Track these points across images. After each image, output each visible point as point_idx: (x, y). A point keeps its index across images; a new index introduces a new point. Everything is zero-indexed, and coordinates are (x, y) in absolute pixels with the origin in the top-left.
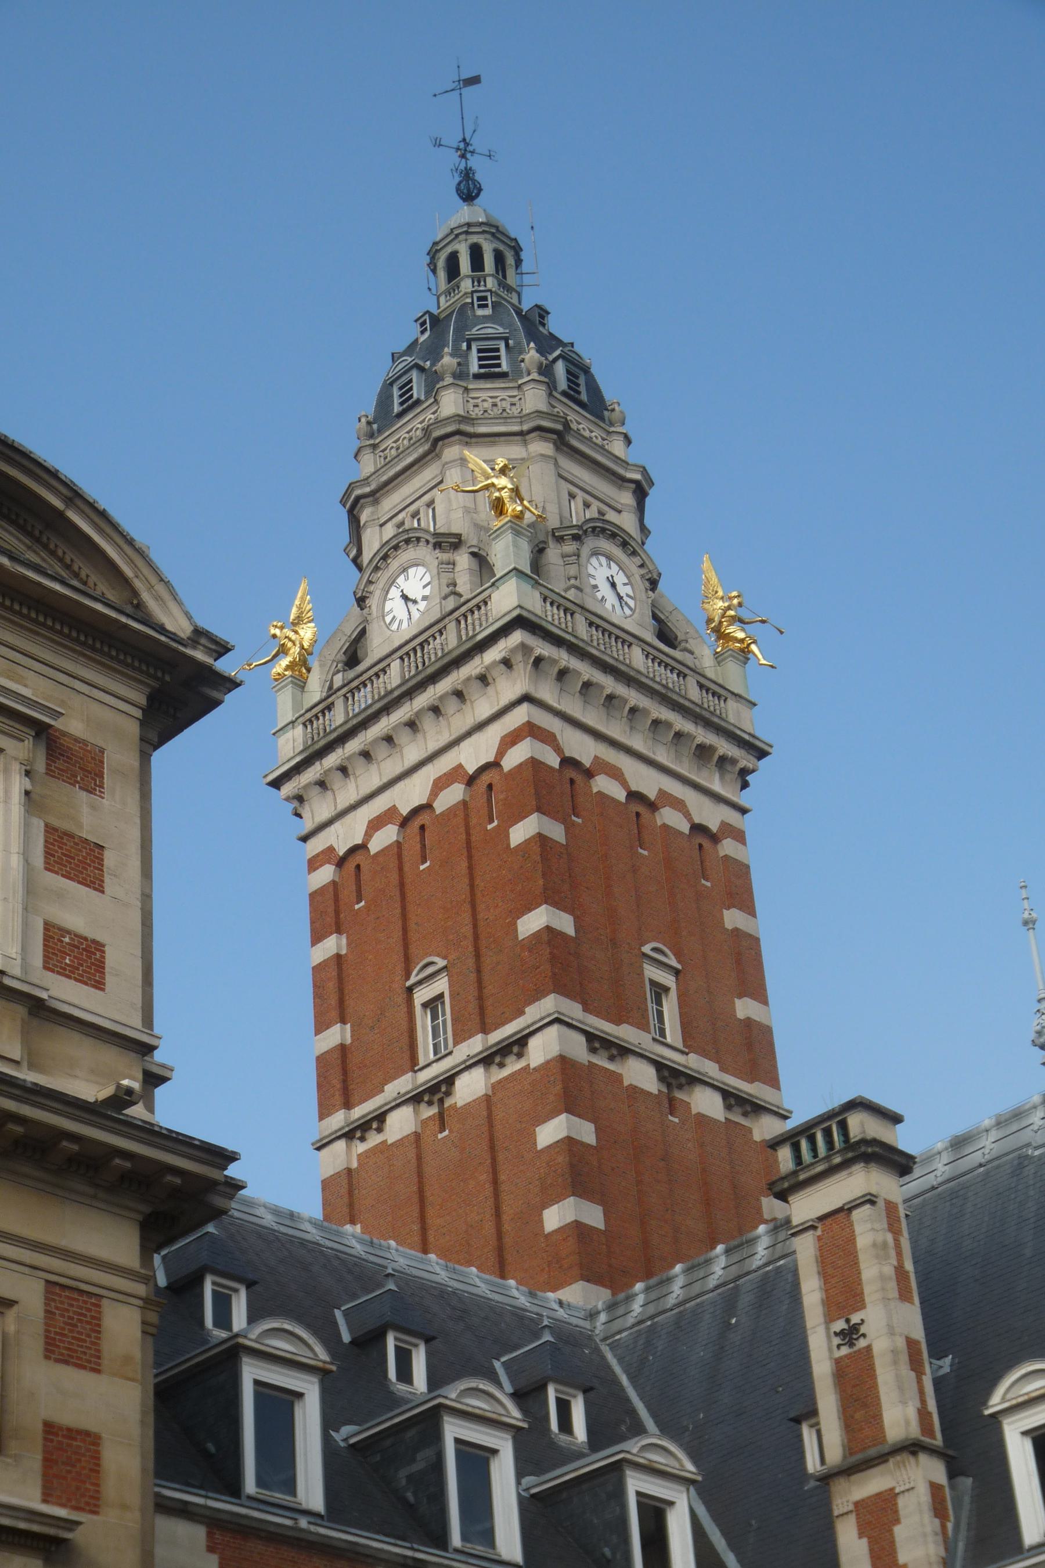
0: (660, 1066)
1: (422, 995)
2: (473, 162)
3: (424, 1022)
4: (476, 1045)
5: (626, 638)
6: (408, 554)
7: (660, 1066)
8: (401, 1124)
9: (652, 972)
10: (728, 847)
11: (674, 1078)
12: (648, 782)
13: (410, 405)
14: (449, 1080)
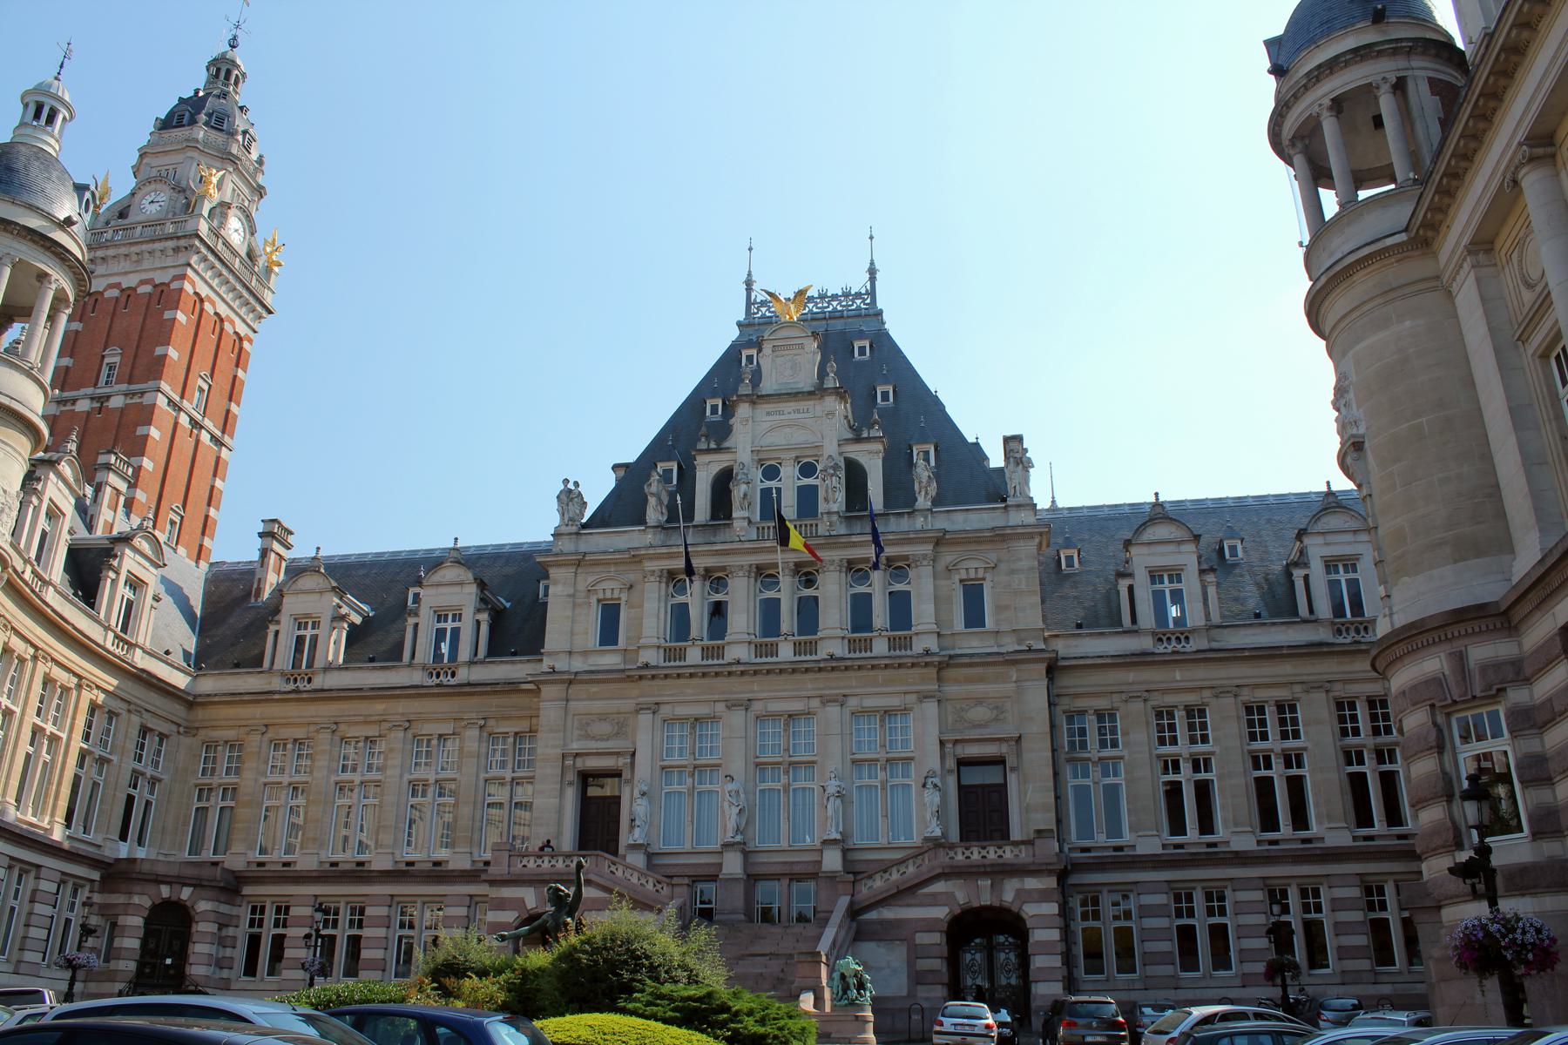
0: (192, 419)
1: (107, 360)
2: (239, 32)
3: (105, 371)
4: (124, 387)
5: (235, 253)
6: (159, 186)
7: (192, 419)
8: (83, 406)
9: (200, 382)
10: (246, 344)
11: (195, 424)
12: (223, 310)
13: (180, 125)
14: (108, 397)
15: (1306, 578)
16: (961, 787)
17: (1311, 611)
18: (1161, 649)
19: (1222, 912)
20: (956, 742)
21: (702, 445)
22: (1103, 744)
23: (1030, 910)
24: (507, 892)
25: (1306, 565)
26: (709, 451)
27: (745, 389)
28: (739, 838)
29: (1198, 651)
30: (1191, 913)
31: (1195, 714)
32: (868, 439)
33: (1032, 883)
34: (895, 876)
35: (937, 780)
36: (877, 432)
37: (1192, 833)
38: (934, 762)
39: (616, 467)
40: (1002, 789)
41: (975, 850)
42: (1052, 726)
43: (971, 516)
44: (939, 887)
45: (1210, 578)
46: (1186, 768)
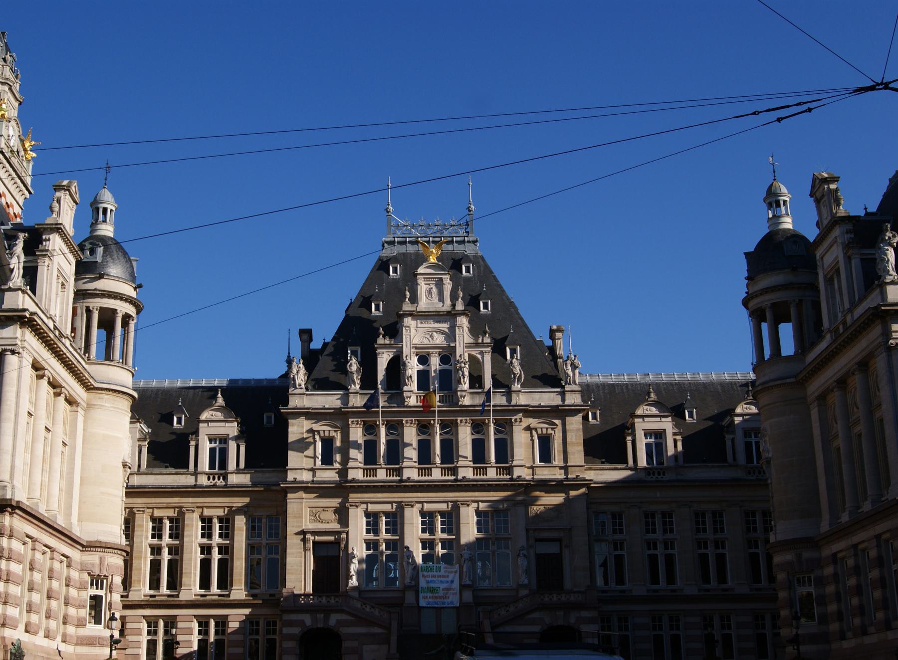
15: (733, 440)
16: (536, 554)
17: (735, 459)
18: (649, 478)
19: (678, 628)
20: (535, 530)
21: (381, 340)
22: (615, 532)
23: (585, 628)
24: (294, 617)
25: (733, 432)
26: (385, 346)
27: (407, 307)
28: (413, 583)
29: (669, 481)
30: (661, 629)
31: (667, 516)
32: (483, 345)
33: (585, 614)
34: (512, 609)
35: (525, 552)
37: (662, 583)
38: (522, 542)
40: (558, 557)
41: (555, 595)
42: (589, 521)
44: (536, 615)
45: (679, 437)
46: (660, 547)
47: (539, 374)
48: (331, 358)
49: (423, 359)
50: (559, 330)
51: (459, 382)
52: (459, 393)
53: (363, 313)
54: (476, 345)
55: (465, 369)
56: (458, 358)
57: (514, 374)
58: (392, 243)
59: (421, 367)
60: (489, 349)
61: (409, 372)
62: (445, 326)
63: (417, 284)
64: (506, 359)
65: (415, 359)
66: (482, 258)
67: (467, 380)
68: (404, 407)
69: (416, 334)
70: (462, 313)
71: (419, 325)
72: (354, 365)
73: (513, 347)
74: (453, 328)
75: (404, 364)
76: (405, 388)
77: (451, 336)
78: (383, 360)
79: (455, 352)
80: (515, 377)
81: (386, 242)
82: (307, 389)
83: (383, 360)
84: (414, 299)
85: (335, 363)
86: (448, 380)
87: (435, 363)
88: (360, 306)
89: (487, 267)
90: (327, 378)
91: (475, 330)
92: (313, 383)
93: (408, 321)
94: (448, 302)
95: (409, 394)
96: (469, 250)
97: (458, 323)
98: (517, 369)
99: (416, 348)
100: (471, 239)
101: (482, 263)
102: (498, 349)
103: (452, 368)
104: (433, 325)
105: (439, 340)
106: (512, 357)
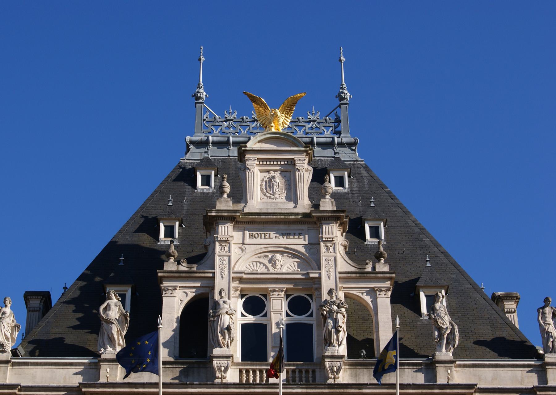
21: (170, 266)
26: (178, 276)
32: (374, 276)
36: (382, 267)
39: (28, 296)
43: (502, 372)
47: (489, 337)
48: (73, 307)
49: (255, 304)
50: (509, 297)
51: (328, 342)
52: (328, 363)
53: (145, 240)
54: (361, 276)
55: (340, 316)
56: (325, 296)
57: (440, 329)
58: (203, 144)
59: (250, 319)
60: (388, 284)
61: (226, 320)
62: (298, 243)
63: (246, 169)
64: (419, 313)
65: (238, 304)
66: (366, 167)
67: (343, 336)
68: (214, 385)
69: (239, 255)
70: (333, 217)
71: (247, 241)
72: (114, 309)
73: (432, 292)
74: (314, 247)
75: (216, 305)
76: (217, 351)
77: (311, 259)
78: (175, 303)
79: (319, 289)
80: (441, 336)
81: (193, 143)
82: (15, 353)
83: (175, 303)
84: (239, 194)
85: (80, 315)
86: (302, 343)
87: (278, 312)
88: (137, 231)
89: (374, 180)
90: (62, 339)
91: (357, 251)
92: (32, 347)
93: (225, 230)
94: (304, 204)
95: (224, 362)
96: (345, 154)
97: (325, 236)
98: (446, 321)
99: (241, 280)
100: (345, 140)
101: (364, 173)
102: (405, 296)
103: (312, 321)
104: (275, 239)
105: (287, 266)
106: (431, 308)
